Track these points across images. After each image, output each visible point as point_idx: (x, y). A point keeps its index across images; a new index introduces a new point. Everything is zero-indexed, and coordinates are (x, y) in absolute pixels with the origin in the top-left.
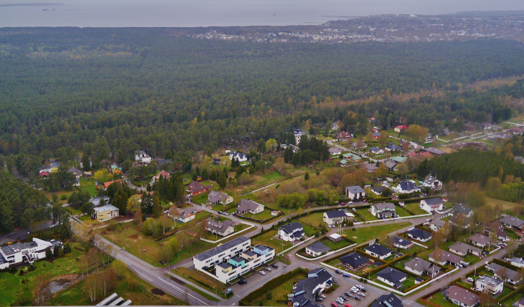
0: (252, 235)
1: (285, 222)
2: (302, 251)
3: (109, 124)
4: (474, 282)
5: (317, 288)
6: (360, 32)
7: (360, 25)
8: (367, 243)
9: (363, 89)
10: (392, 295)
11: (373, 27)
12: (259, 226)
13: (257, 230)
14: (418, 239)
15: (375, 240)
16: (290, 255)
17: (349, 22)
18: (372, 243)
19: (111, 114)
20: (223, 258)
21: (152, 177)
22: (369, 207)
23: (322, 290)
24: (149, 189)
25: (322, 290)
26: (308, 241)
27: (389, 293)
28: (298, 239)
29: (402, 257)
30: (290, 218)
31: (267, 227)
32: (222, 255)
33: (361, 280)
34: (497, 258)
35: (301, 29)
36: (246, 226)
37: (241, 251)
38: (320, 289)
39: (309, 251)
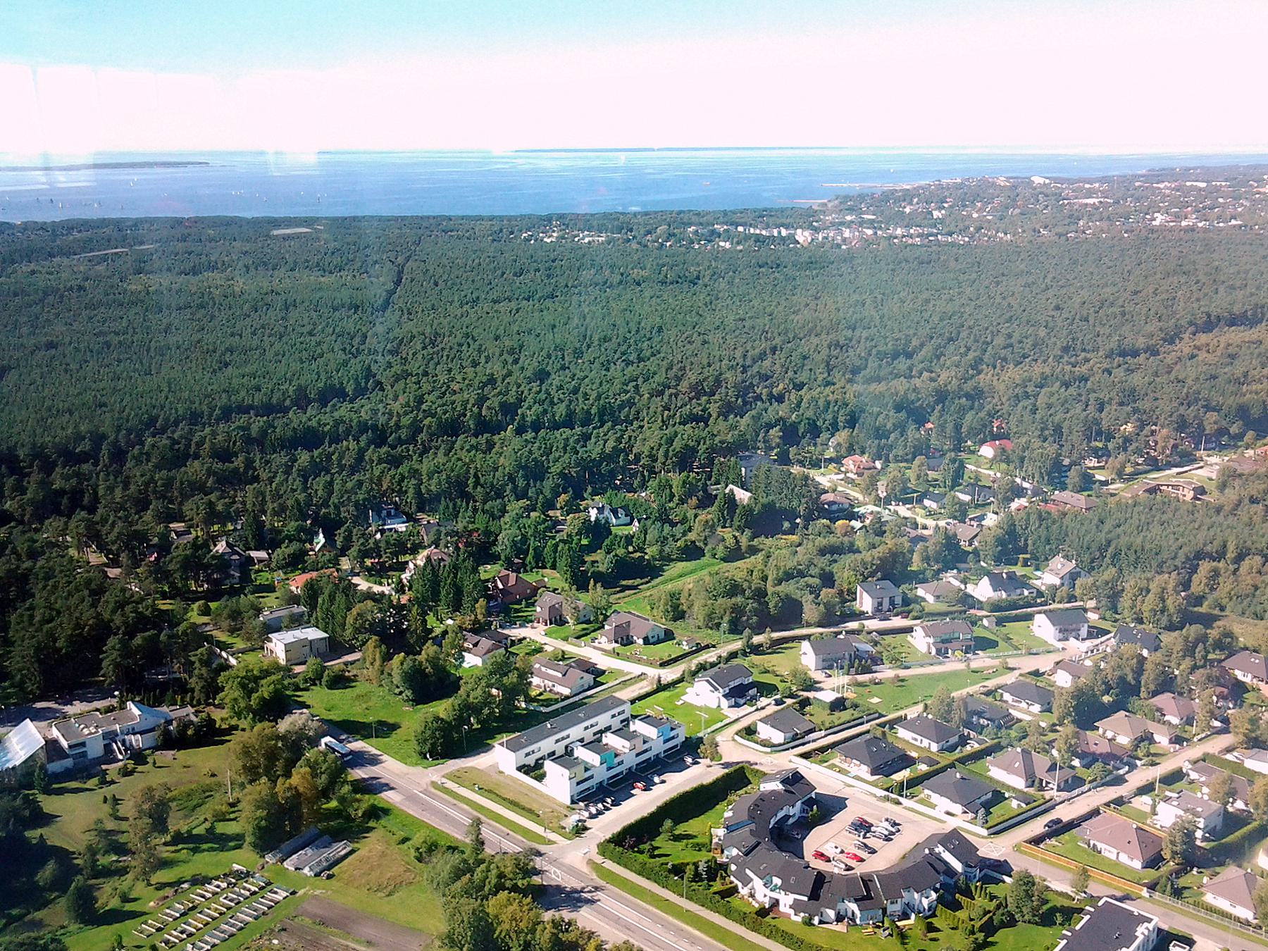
0: (635, 695)
1: (713, 665)
2: (750, 732)
3: (310, 439)
4: (1154, 807)
5: (781, 815)
6: (908, 222)
7: (911, 203)
8: (902, 713)
9: (909, 356)
10: (955, 833)
11: (940, 208)
12: (653, 672)
13: (645, 683)
14: (1023, 705)
15: (920, 707)
16: (719, 738)
17: (887, 197)
18: (912, 712)
19: (313, 417)
20: (566, 747)
21: (407, 563)
22: (909, 630)
23: (791, 821)
24: (400, 589)
25: (791, 821)
26: (763, 708)
27: (947, 828)
28: (742, 701)
29: (983, 746)
30: (724, 654)
31: (669, 675)
32: (563, 739)
33: (887, 799)
34: (1211, 751)
35: (763, 215)
36: (621, 673)
37: (608, 729)
38: (787, 817)
39: (765, 731)
